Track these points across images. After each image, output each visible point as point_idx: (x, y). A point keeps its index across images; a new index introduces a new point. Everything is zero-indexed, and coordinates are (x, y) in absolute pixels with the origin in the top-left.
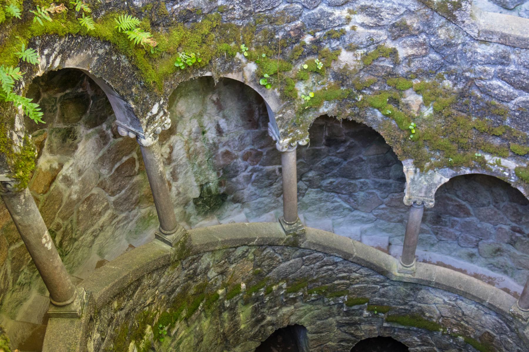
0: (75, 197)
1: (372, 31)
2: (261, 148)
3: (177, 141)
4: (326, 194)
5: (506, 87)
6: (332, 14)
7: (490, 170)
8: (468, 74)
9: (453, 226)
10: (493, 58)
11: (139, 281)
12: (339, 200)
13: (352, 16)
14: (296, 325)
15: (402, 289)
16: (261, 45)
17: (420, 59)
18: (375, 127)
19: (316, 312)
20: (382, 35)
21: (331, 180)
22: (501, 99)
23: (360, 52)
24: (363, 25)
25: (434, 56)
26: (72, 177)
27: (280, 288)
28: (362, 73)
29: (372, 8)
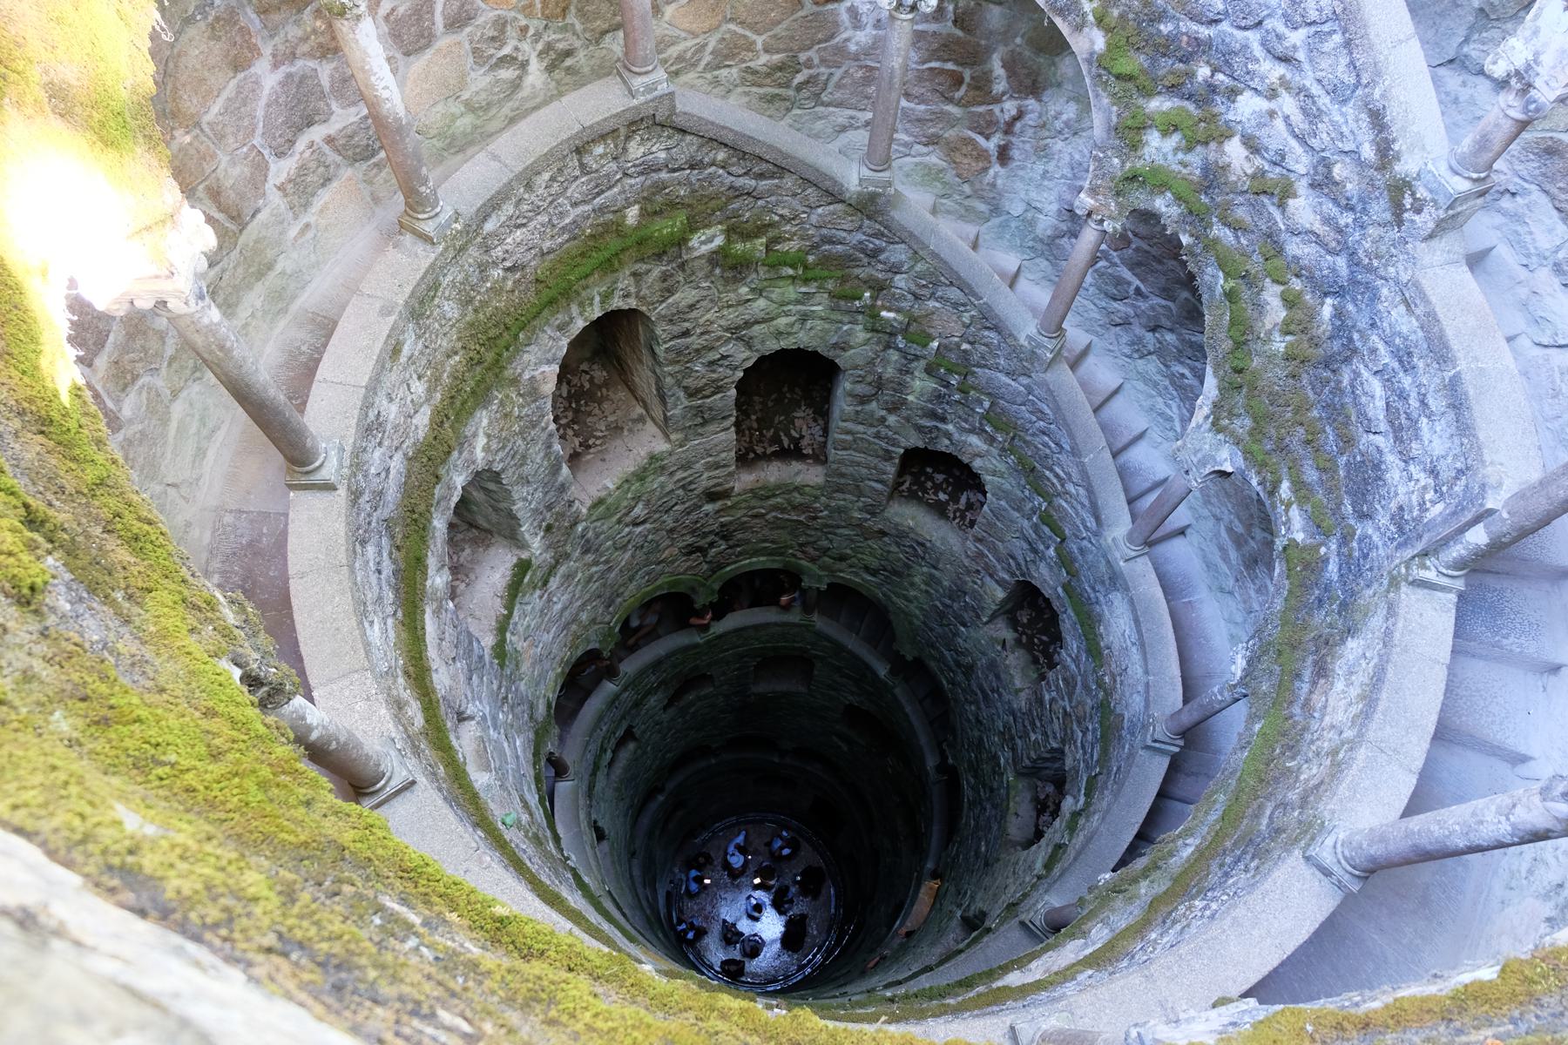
0: (853, 48)
1: (1293, 143)
2: (1136, 235)
3: (1032, 111)
4: (1167, 383)
5: (1381, 404)
6: (1257, 61)
7: (1274, 507)
8: (1356, 336)
9: (1258, 591)
10: (1397, 341)
11: (780, 170)
12: (1175, 409)
13: (1282, 91)
14: (977, 476)
15: (1103, 567)
16: (1131, 16)
17: (1323, 252)
18: (1205, 298)
19: (1007, 486)
20: (1300, 162)
21: (1187, 372)
22: (1362, 414)
23: (1258, 161)
24: (1287, 118)
25: (1341, 262)
26: (864, 19)
27: (980, 403)
28: (1241, 199)
29: (1314, 103)
